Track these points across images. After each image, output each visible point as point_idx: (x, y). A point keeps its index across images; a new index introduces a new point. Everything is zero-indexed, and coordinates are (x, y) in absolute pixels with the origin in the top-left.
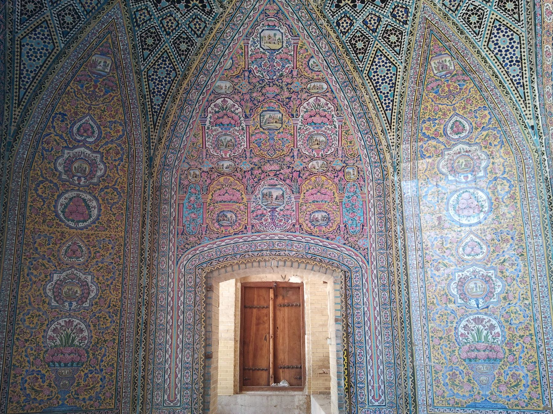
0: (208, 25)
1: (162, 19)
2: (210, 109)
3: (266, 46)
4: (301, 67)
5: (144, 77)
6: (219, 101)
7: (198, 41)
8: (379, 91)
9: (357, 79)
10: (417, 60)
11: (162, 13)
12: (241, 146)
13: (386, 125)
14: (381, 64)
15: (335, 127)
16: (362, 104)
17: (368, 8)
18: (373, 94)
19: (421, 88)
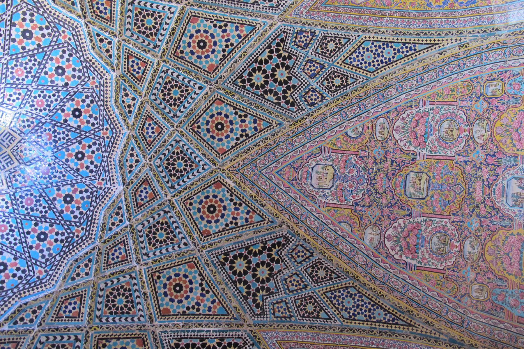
0: (301, 243)
1: (288, 290)
2: (396, 257)
3: (329, 184)
4: (356, 147)
5: (349, 324)
6: (388, 244)
7: (317, 256)
8: (392, 59)
9: (376, 84)
10: (355, 19)
11: (282, 289)
12: (447, 226)
13: (434, 50)
14: (360, 58)
15: (431, 109)
16: (406, 78)
17: (297, 73)
18: (395, 66)
19: (388, 12)
